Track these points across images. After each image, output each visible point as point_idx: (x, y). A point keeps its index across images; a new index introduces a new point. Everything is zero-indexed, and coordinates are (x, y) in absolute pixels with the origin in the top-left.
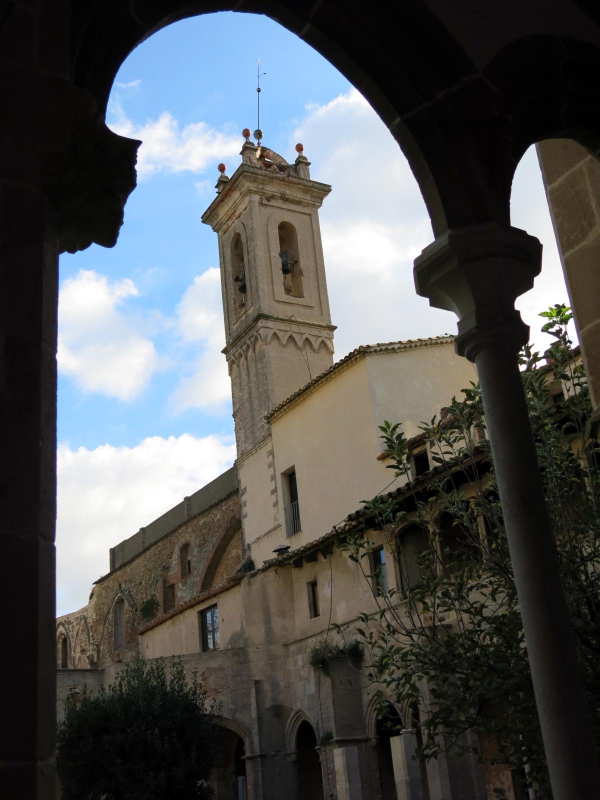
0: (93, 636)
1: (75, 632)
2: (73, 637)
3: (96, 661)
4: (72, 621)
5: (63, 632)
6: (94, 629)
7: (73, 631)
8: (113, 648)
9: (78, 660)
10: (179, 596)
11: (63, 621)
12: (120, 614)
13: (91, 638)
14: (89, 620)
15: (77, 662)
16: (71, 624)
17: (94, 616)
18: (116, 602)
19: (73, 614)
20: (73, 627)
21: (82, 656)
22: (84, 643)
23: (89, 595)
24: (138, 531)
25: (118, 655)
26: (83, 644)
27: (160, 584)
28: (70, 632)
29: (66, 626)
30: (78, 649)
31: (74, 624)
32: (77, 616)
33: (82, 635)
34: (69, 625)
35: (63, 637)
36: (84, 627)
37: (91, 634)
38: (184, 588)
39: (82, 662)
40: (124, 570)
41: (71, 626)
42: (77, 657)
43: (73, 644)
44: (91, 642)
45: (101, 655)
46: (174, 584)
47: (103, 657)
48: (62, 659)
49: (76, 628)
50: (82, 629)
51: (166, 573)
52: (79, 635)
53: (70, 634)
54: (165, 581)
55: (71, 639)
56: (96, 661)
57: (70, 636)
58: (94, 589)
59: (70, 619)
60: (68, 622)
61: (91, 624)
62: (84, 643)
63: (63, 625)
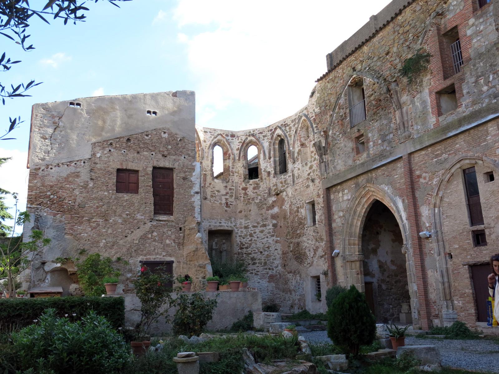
0: (317, 127)
1: (293, 133)
2: (290, 136)
3: (324, 145)
4: (289, 123)
5: (280, 134)
6: (317, 121)
7: (290, 131)
8: (349, 126)
9: (298, 153)
10: (469, 32)
11: (280, 125)
12: (353, 97)
13: (315, 129)
14: (310, 115)
15: (296, 155)
16: (288, 126)
17: (317, 110)
18: (349, 86)
19: (290, 117)
20: (290, 128)
21: (302, 149)
22: (303, 139)
23: (310, 94)
24: (368, 20)
25: (359, 130)
26: (302, 139)
27: (432, 32)
28: (287, 132)
29: (283, 128)
30: (298, 144)
31: (292, 125)
32: (293, 118)
33: (301, 132)
34: (286, 127)
35: (280, 139)
36: (303, 125)
37: (314, 126)
38: (481, 20)
39: (302, 154)
40: (361, 50)
41: (287, 128)
42: (297, 150)
43: (291, 142)
44: (316, 131)
45: (330, 139)
46: (456, 27)
47: (334, 139)
48: (279, 157)
49: (294, 129)
50: (301, 127)
51: (439, 20)
52: (298, 132)
53: (287, 134)
54: (439, 30)
55: (289, 138)
56: (324, 145)
57: (288, 136)
58: (315, 87)
59: (286, 123)
60: (285, 125)
61: (314, 117)
62: (303, 139)
63: (280, 128)
